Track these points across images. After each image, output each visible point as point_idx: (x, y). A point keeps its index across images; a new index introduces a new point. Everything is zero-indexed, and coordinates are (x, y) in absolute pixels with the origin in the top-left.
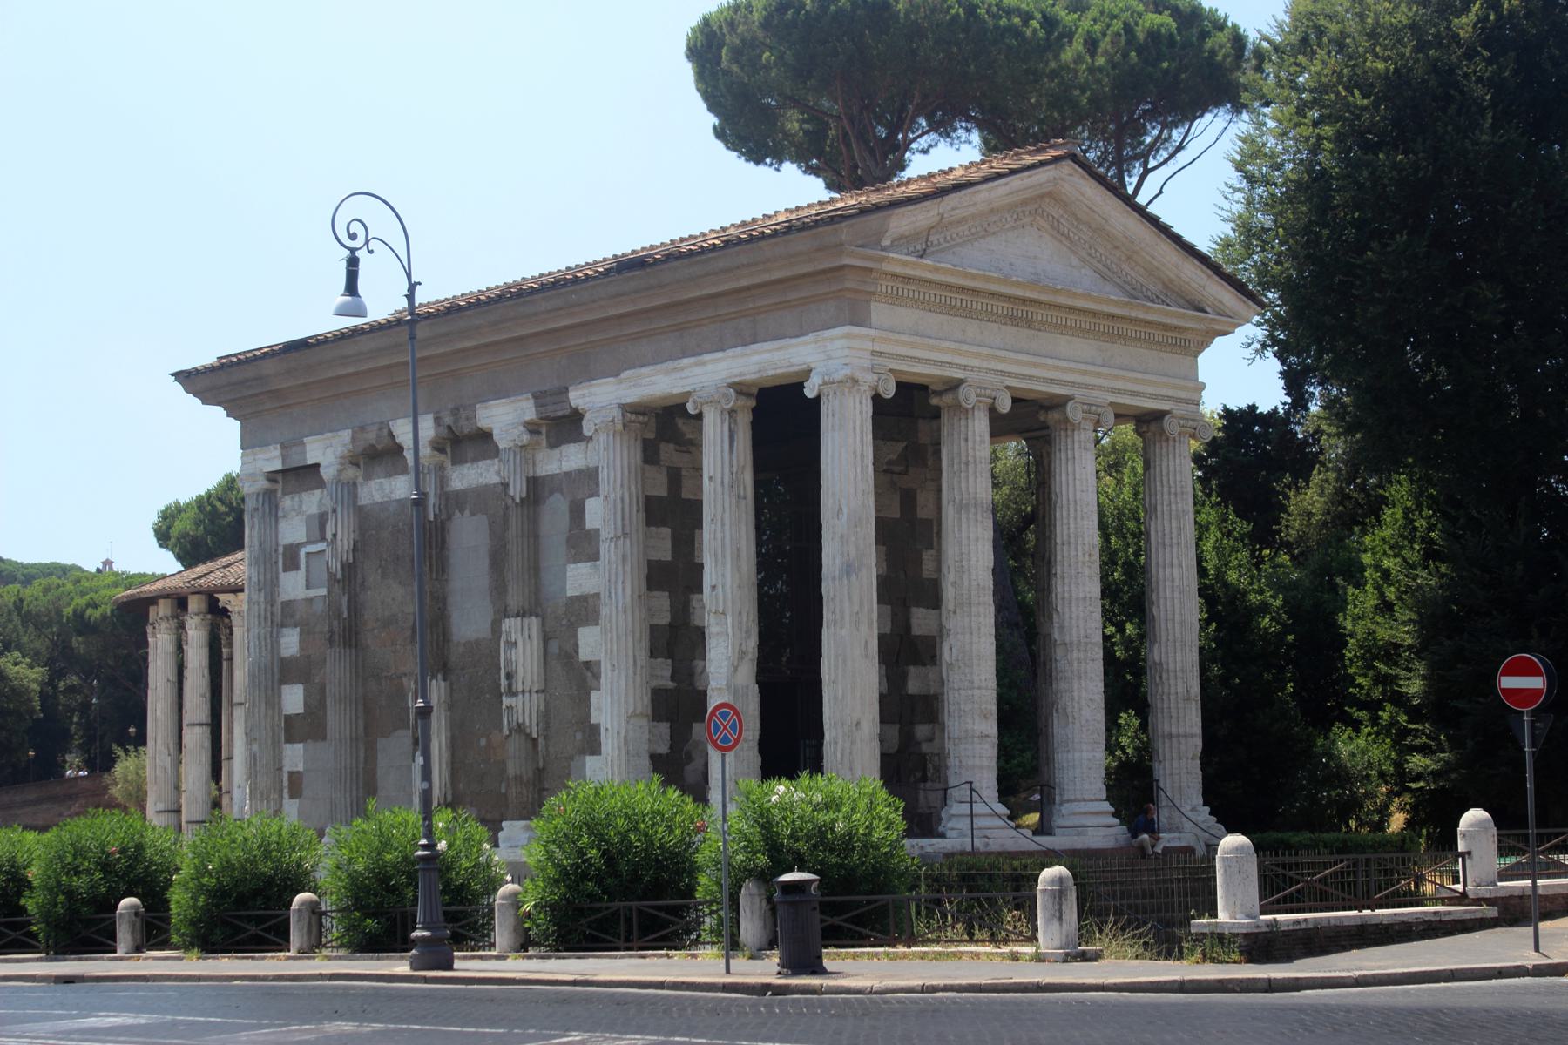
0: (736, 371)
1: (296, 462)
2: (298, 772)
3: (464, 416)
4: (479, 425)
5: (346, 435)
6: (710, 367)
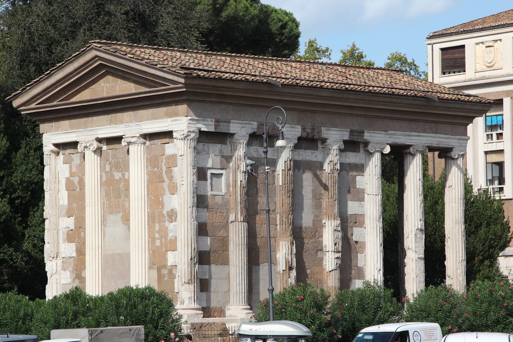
0: (430, 142)
1: (223, 129)
2: (206, 279)
3: (316, 131)
4: (323, 136)
5: (255, 124)
6: (420, 138)
